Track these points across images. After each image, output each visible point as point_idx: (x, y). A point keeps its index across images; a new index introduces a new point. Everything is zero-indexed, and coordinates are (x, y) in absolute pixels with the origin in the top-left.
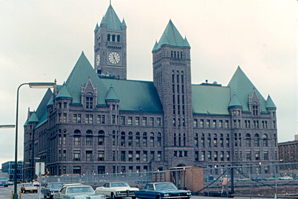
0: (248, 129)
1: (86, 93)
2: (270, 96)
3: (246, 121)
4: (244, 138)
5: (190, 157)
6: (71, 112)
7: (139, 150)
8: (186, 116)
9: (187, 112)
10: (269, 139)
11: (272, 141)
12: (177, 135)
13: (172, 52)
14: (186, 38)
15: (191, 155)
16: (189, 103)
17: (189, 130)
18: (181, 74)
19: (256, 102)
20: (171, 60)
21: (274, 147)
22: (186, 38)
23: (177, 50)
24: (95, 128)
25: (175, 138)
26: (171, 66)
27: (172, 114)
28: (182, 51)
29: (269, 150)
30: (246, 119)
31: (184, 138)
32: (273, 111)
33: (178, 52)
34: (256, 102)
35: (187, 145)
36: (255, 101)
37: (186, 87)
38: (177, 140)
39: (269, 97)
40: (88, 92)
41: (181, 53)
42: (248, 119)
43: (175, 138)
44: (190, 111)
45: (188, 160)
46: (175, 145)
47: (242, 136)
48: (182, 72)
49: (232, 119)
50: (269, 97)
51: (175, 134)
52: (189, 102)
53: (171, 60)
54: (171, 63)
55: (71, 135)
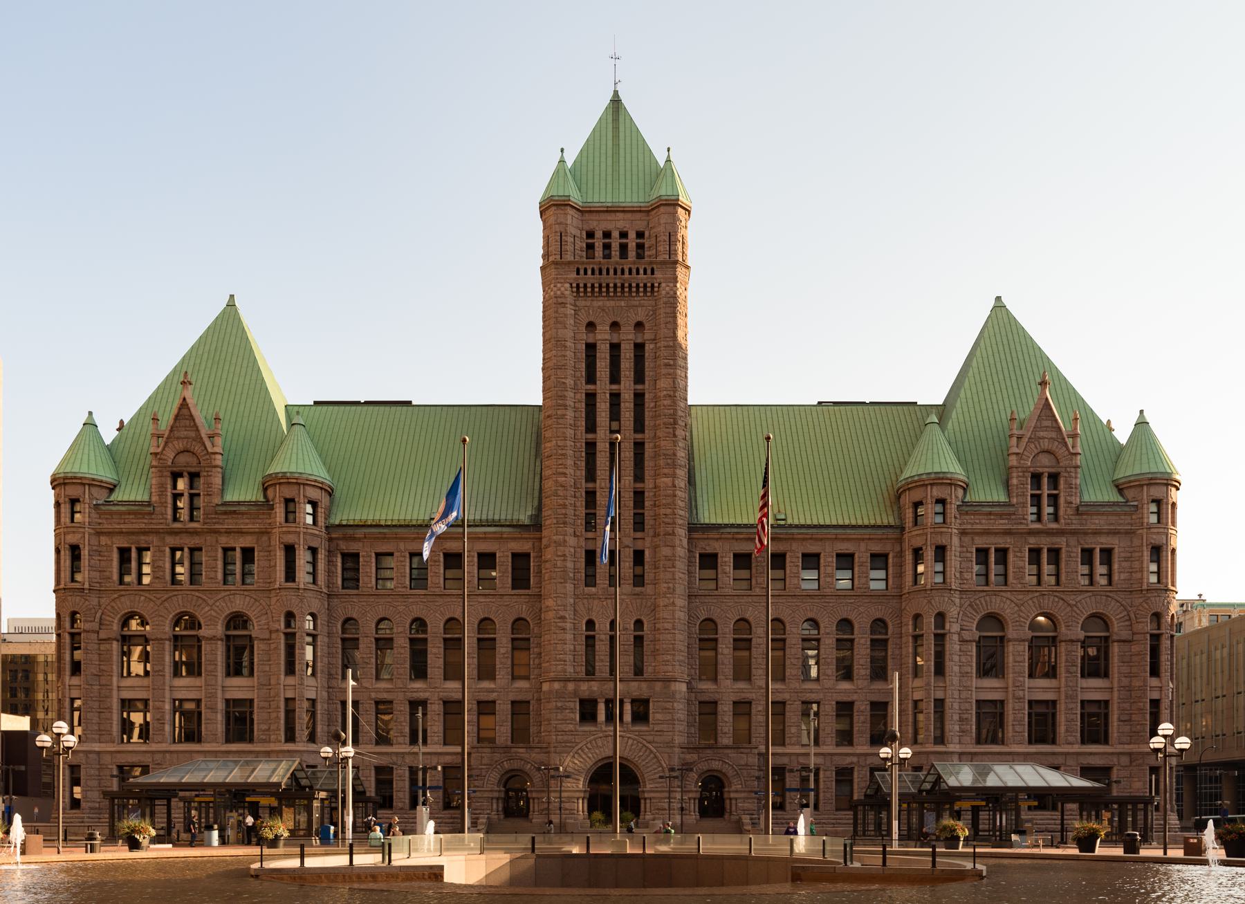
0: (995, 593)
1: (170, 454)
2: (1148, 417)
3: (982, 554)
4: (966, 635)
5: (665, 727)
6: (104, 540)
7: (422, 696)
8: (648, 540)
9: (656, 517)
10: (1118, 641)
11: (1135, 648)
12: (602, 627)
13: (590, 235)
14: (668, 161)
15: (668, 717)
16: (666, 475)
17: (662, 602)
18: (627, 337)
19: (1048, 452)
20: (578, 273)
21: (1145, 681)
22: (668, 161)
23: (615, 224)
24: (210, 602)
25: (590, 641)
26: (581, 303)
27: (581, 529)
28: (640, 226)
29: (1116, 694)
30: (981, 542)
31: (639, 640)
32: (1156, 492)
33: (624, 235)
34: (1048, 452)
35: (648, 670)
36: (1045, 444)
37: (656, 399)
38: (602, 648)
39: (1142, 424)
40: (180, 445)
41: (640, 235)
42: (992, 543)
43: (590, 641)
44: (668, 511)
45: (650, 738)
46: (590, 672)
47: (952, 627)
48: (639, 325)
49: (906, 545)
50: (1142, 424)
51: (590, 624)
52: (666, 471)
53: (578, 273)
54: (578, 286)
55: (103, 635)
